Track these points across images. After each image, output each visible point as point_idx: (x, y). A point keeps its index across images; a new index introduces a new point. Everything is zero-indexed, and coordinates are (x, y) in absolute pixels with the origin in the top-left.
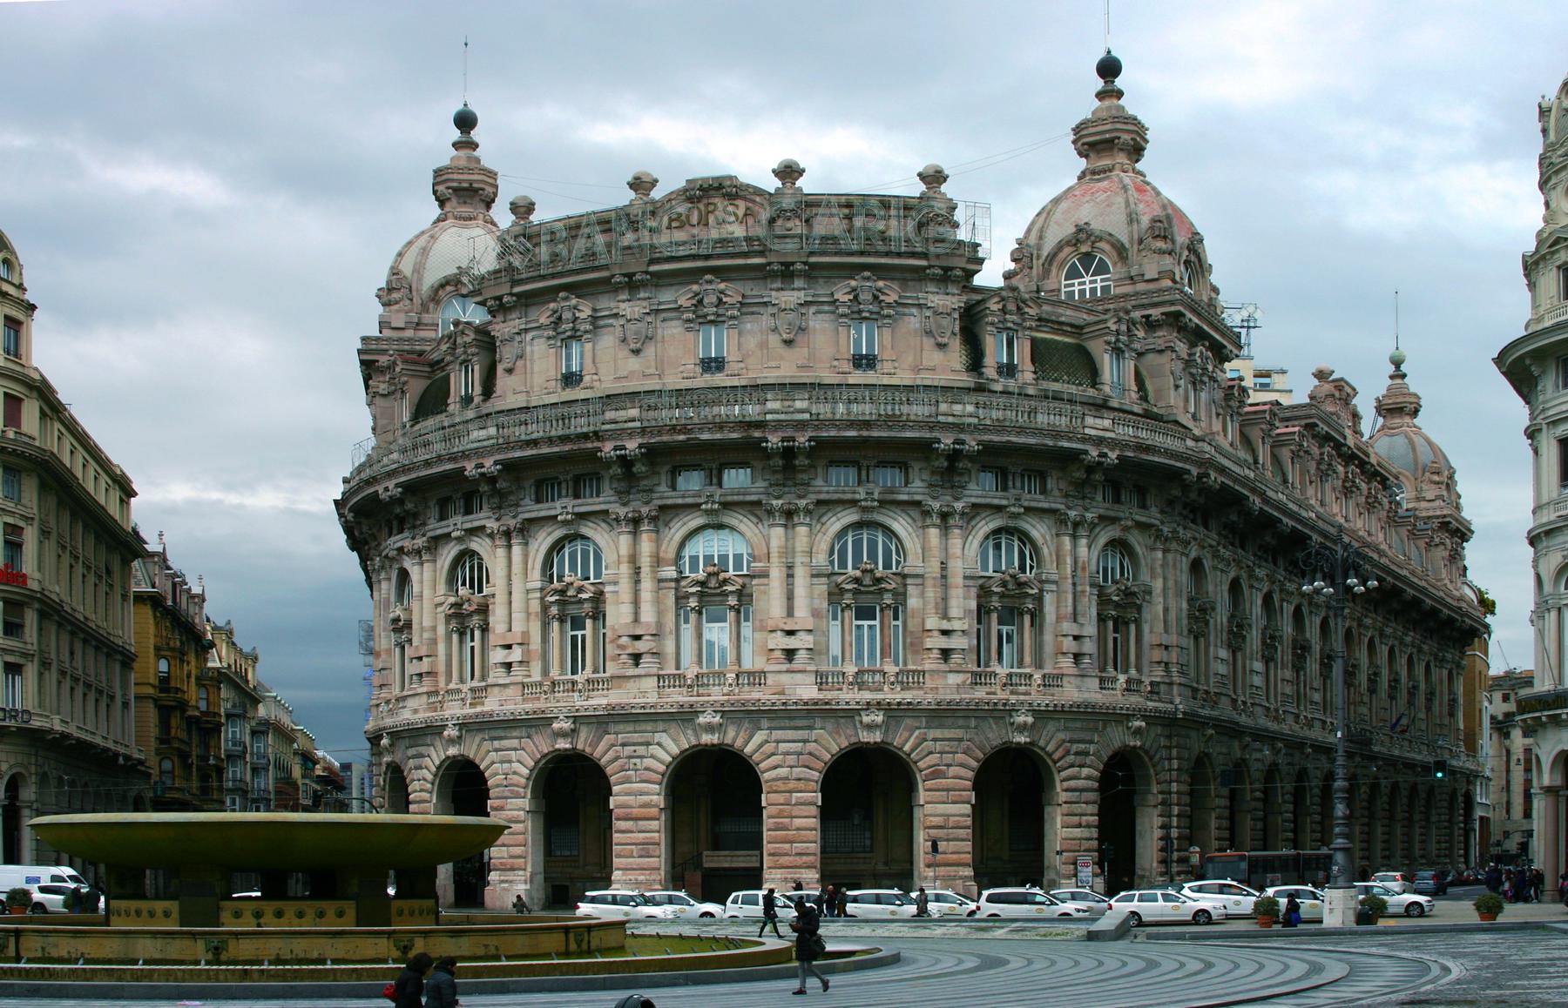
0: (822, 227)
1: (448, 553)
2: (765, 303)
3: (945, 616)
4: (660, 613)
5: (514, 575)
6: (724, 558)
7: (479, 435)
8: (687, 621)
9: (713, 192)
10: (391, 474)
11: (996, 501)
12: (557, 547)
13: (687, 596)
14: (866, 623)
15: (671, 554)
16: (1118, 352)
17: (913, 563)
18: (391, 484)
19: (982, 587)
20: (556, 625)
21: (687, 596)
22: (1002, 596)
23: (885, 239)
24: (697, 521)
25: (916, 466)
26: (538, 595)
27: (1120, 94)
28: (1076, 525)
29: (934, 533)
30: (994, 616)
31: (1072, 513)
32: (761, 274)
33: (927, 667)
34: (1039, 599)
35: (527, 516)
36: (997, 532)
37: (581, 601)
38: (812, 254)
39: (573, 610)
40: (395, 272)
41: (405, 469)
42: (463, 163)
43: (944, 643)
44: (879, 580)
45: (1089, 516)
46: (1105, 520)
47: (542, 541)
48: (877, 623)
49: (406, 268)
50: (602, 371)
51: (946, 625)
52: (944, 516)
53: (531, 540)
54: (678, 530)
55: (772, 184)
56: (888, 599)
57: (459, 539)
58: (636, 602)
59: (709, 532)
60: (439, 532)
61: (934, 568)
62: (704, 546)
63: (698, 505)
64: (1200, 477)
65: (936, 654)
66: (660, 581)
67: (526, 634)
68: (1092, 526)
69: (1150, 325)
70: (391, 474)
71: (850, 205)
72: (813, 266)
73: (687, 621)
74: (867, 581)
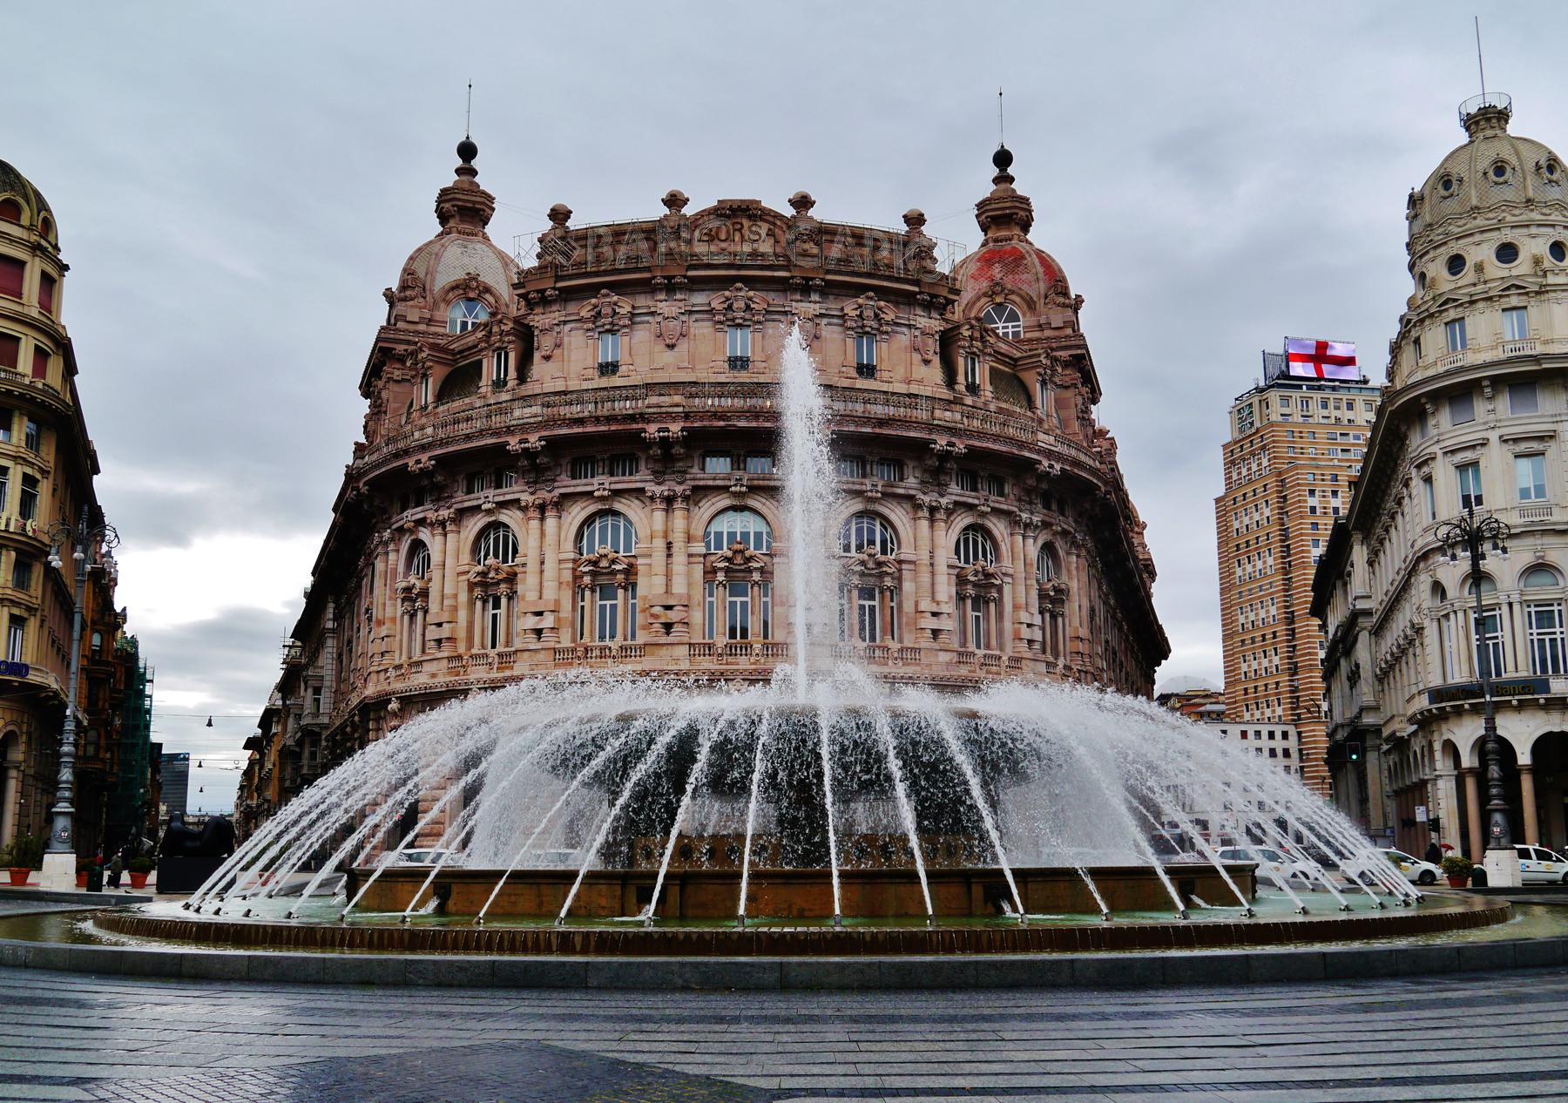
0: (835, 251)
1: (474, 525)
2: (785, 313)
3: (933, 599)
4: (689, 585)
5: (546, 545)
6: (745, 535)
7: (520, 413)
8: (711, 595)
9: (739, 213)
10: (423, 448)
11: (970, 501)
12: (589, 521)
13: (714, 571)
14: (867, 603)
15: (701, 533)
16: (1044, 383)
17: (907, 552)
18: (424, 457)
19: (958, 576)
20: (587, 593)
21: (714, 571)
22: (975, 585)
23: (889, 266)
24: (726, 502)
25: (911, 464)
26: (571, 565)
27: (1012, 180)
28: (1027, 526)
29: (924, 524)
31: (1024, 516)
32: (783, 286)
33: (923, 645)
34: (1000, 589)
35: (563, 491)
36: (966, 529)
37: (614, 573)
38: (828, 272)
39: (603, 580)
40: (408, 272)
41: (443, 443)
42: (466, 186)
43: (933, 623)
44: (879, 564)
45: (1035, 519)
46: (1046, 525)
47: (577, 513)
48: (876, 603)
49: (421, 274)
50: (638, 360)
51: (935, 610)
52: (933, 510)
53: (564, 514)
54: (708, 507)
55: (789, 212)
56: (888, 582)
57: (489, 512)
58: (668, 576)
59: (731, 514)
60: (467, 504)
61: (924, 557)
62: (725, 525)
63: (726, 489)
64: (1107, 492)
65: (929, 634)
66: (690, 556)
67: (557, 602)
68: (1036, 527)
69: (1066, 365)
70: (423, 448)
71: (858, 236)
72: (829, 283)
73: (711, 595)
74: (871, 565)
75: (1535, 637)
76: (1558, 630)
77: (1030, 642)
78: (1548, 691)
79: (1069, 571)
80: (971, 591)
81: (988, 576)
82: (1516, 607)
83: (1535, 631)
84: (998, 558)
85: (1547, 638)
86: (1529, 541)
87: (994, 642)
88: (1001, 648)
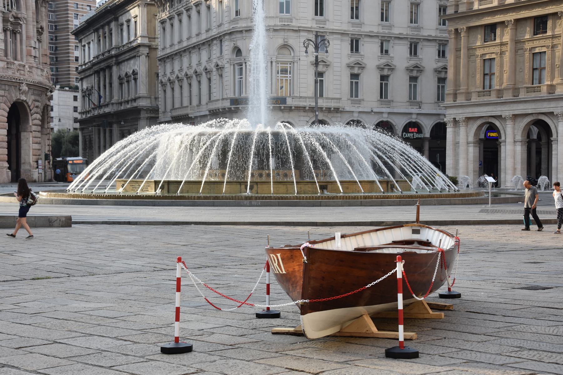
19: (3, 17)
22: (12, 23)
30: (8, 33)
75: (279, 78)
76: (289, 75)
77: (35, 57)
78: (285, 103)
79: (41, 16)
80: (10, 27)
81: (16, 18)
82: (274, 64)
83: (279, 75)
84: (18, 8)
85: (284, 79)
86: (282, 33)
87: (19, 57)
88: (22, 60)
